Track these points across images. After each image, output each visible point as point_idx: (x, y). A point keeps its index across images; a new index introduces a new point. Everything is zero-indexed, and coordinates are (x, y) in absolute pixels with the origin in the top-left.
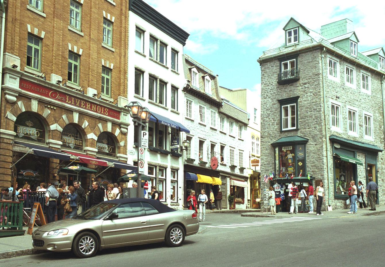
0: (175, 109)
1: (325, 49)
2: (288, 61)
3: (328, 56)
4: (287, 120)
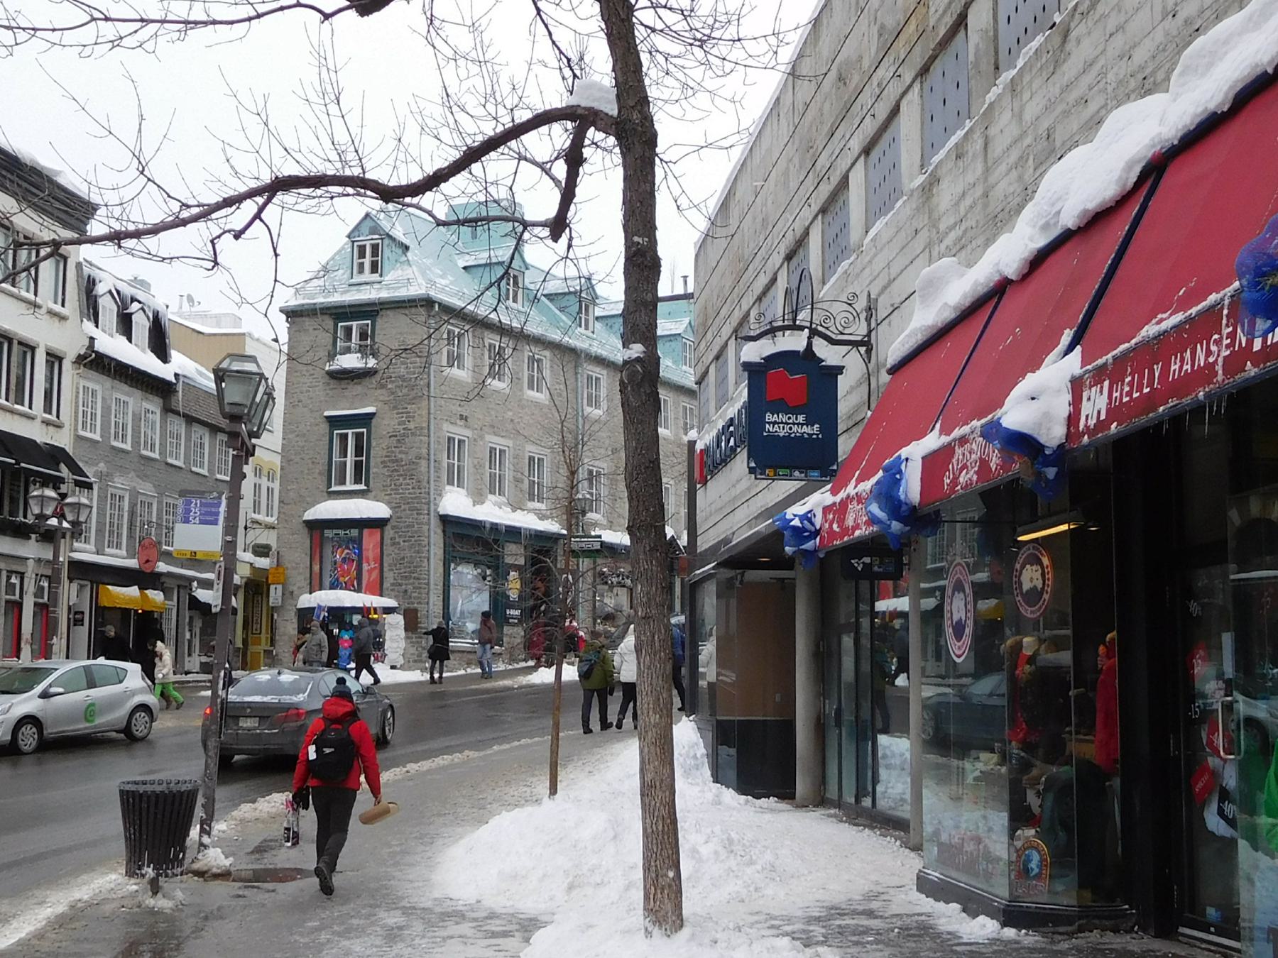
0: (50, 413)
2: (354, 324)
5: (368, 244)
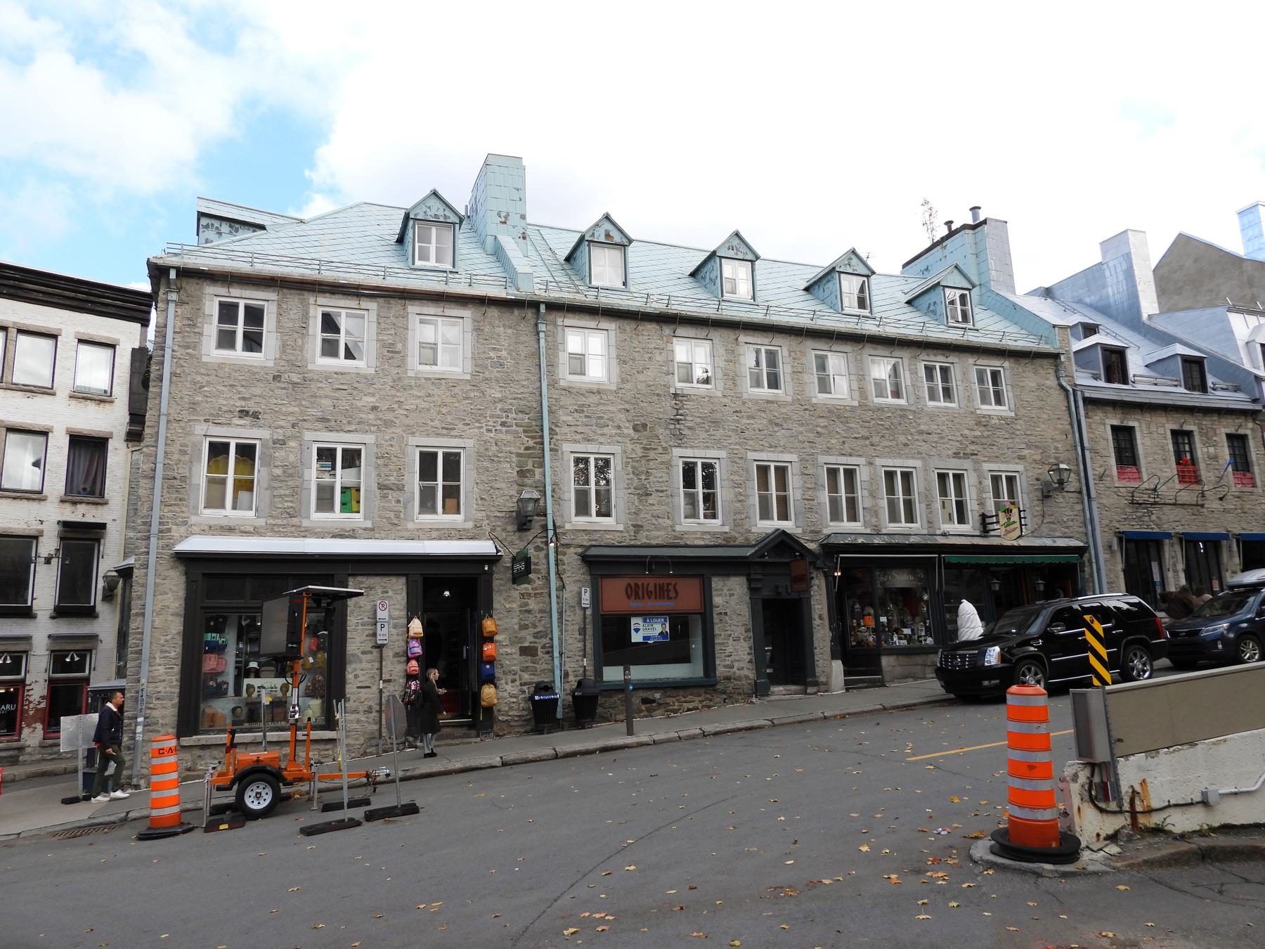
1: (173, 274)
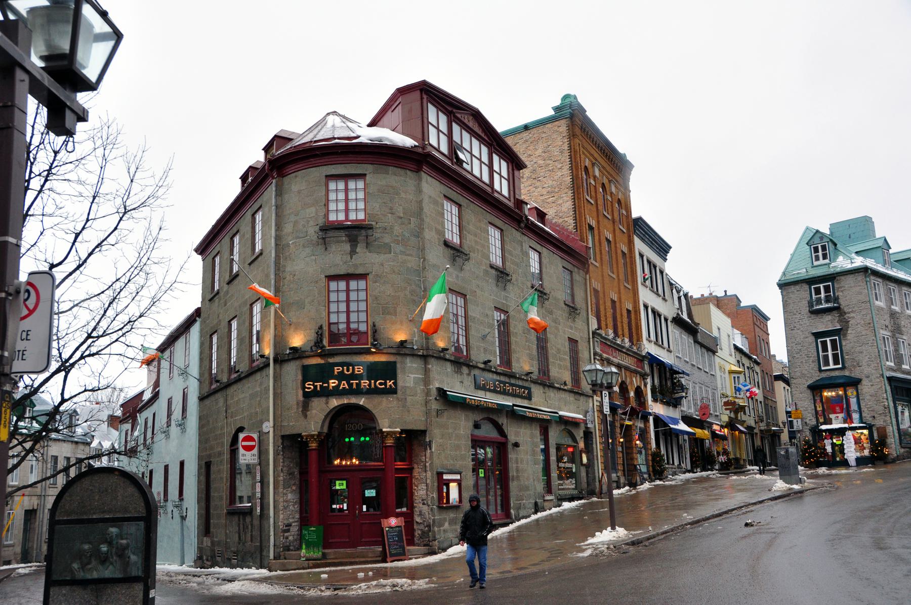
2: (821, 286)
3: (872, 277)
4: (828, 355)
5: (819, 246)
